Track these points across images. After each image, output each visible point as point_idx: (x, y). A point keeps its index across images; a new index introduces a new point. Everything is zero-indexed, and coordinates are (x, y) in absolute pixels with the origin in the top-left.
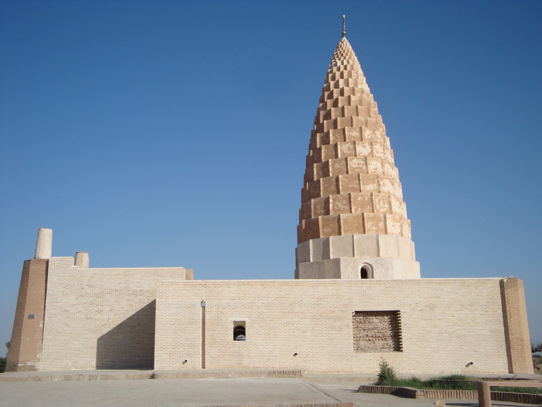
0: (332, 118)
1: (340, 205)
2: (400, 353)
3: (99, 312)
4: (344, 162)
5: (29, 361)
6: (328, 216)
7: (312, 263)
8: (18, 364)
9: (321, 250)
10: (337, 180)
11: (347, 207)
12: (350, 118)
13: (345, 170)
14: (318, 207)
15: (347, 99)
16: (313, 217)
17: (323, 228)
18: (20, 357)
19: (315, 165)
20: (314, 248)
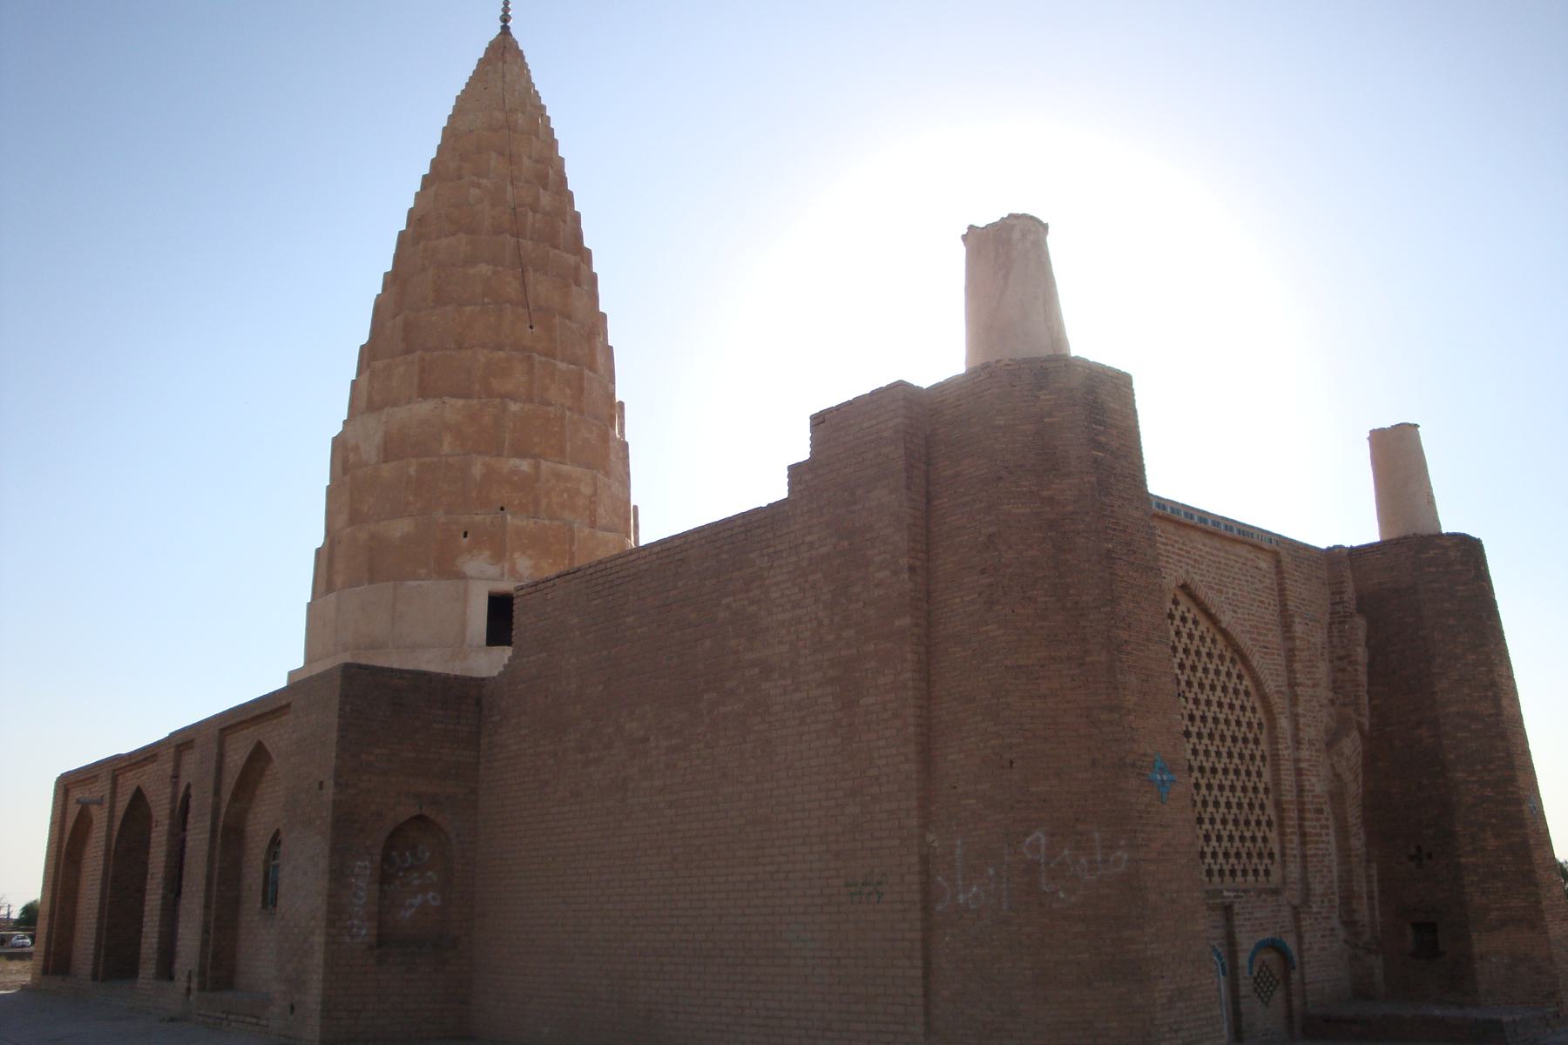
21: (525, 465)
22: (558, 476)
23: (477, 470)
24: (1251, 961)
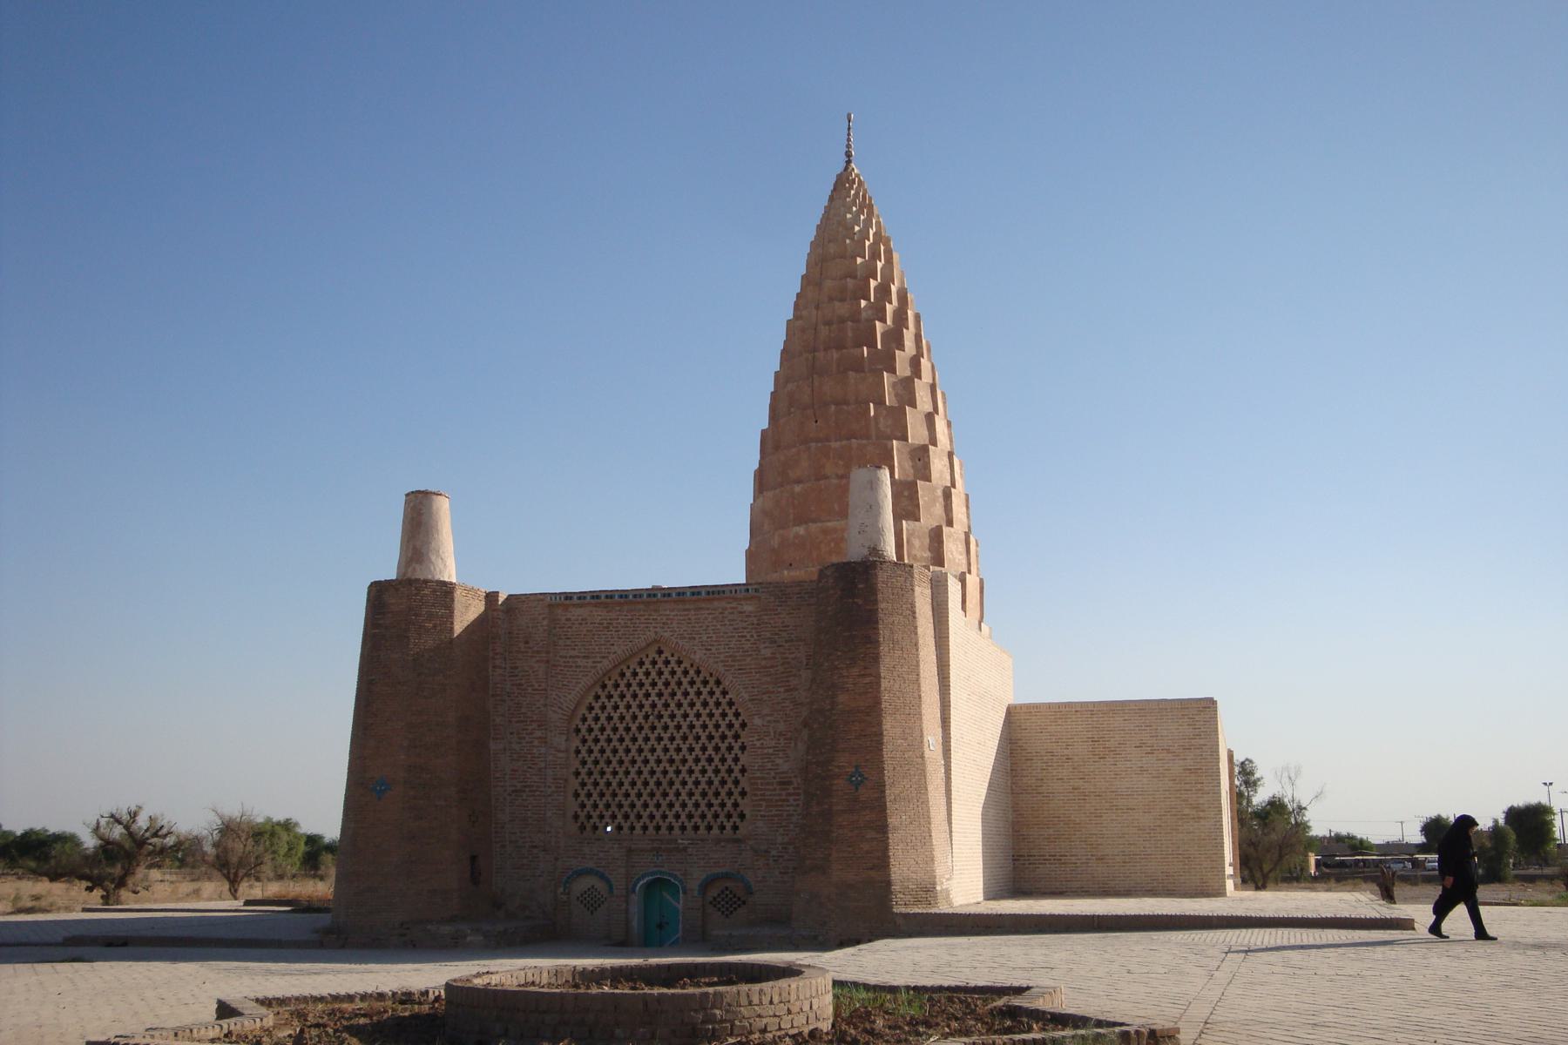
8: (934, 884)
14: (917, 543)
21: (801, 530)
22: (825, 532)
23: (775, 542)
24: (705, 886)
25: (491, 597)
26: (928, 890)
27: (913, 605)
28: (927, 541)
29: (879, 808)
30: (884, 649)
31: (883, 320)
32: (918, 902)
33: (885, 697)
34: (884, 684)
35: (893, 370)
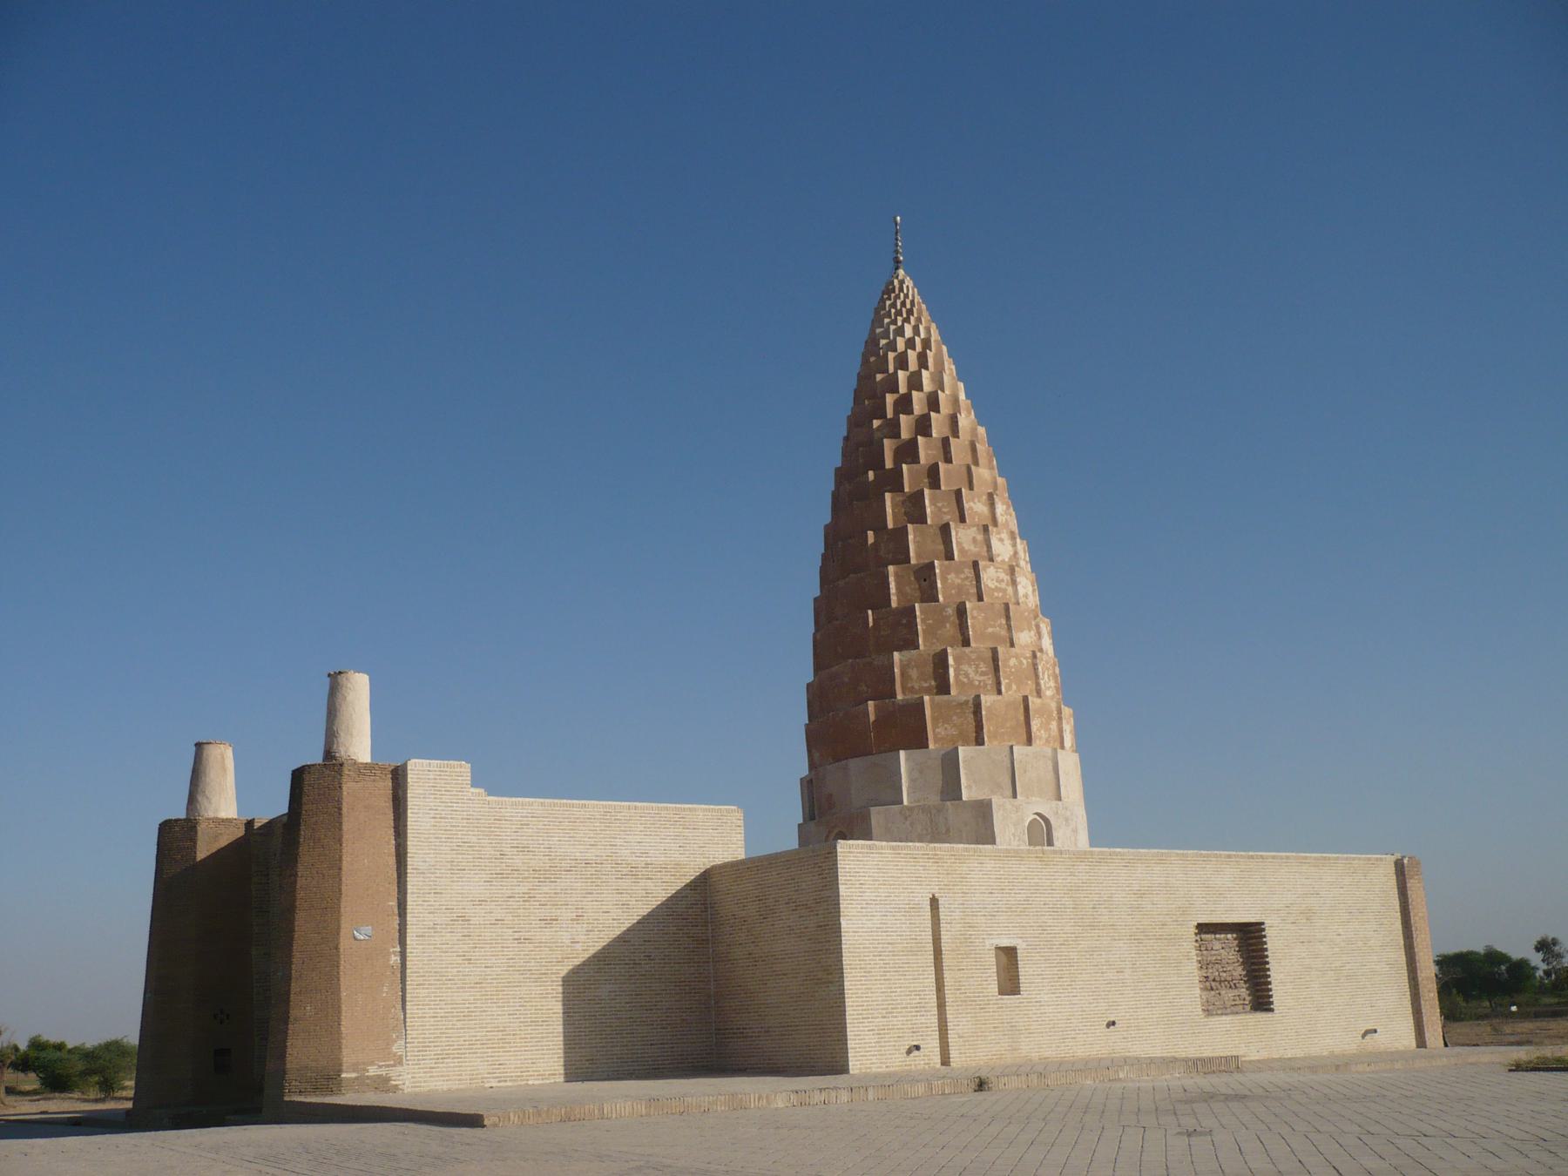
0: (923, 460)
1: (972, 675)
2: (1270, 1015)
3: (549, 922)
4: (969, 572)
5: (372, 1063)
6: (945, 697)
7: (910, 809)
8: (340, 1071)
9: (936, 778)
10: (961, 612)
11: (989, 680)
12: (964, 469)
13: (974, 590)
14: (914, 673)
15: (947, 422)
16: (900, 697)
17: (935, 726)
18: (345, 1052)
19: (891, 568)
20: (910, 772)
25: (249, 824)
26: (330, 1079)
27: (339, 802)
28: (930, 669)
29: (286, 1001)
30: (303, 849)
31: (897, 435)
32: (316, 1090)
33: (300, 894)
34: (300, 882)
35: (897, 487)
